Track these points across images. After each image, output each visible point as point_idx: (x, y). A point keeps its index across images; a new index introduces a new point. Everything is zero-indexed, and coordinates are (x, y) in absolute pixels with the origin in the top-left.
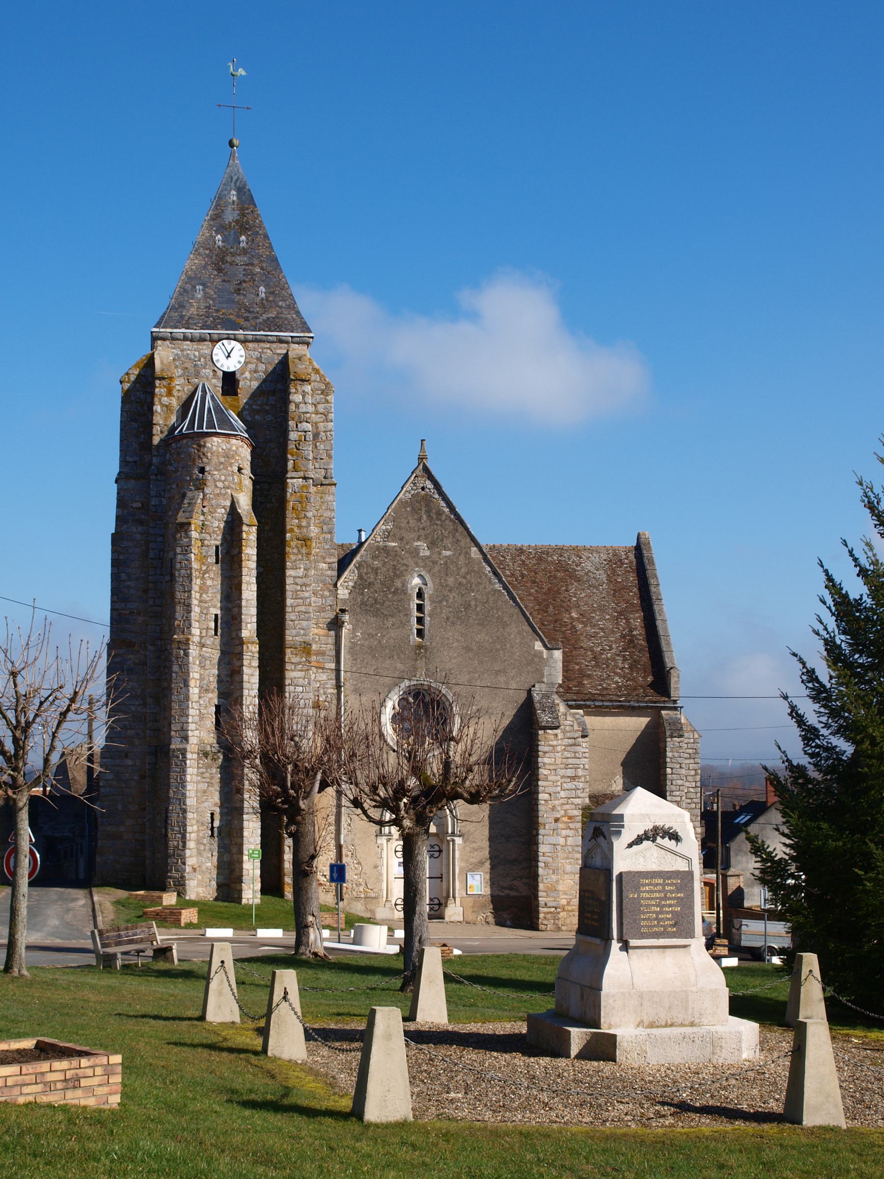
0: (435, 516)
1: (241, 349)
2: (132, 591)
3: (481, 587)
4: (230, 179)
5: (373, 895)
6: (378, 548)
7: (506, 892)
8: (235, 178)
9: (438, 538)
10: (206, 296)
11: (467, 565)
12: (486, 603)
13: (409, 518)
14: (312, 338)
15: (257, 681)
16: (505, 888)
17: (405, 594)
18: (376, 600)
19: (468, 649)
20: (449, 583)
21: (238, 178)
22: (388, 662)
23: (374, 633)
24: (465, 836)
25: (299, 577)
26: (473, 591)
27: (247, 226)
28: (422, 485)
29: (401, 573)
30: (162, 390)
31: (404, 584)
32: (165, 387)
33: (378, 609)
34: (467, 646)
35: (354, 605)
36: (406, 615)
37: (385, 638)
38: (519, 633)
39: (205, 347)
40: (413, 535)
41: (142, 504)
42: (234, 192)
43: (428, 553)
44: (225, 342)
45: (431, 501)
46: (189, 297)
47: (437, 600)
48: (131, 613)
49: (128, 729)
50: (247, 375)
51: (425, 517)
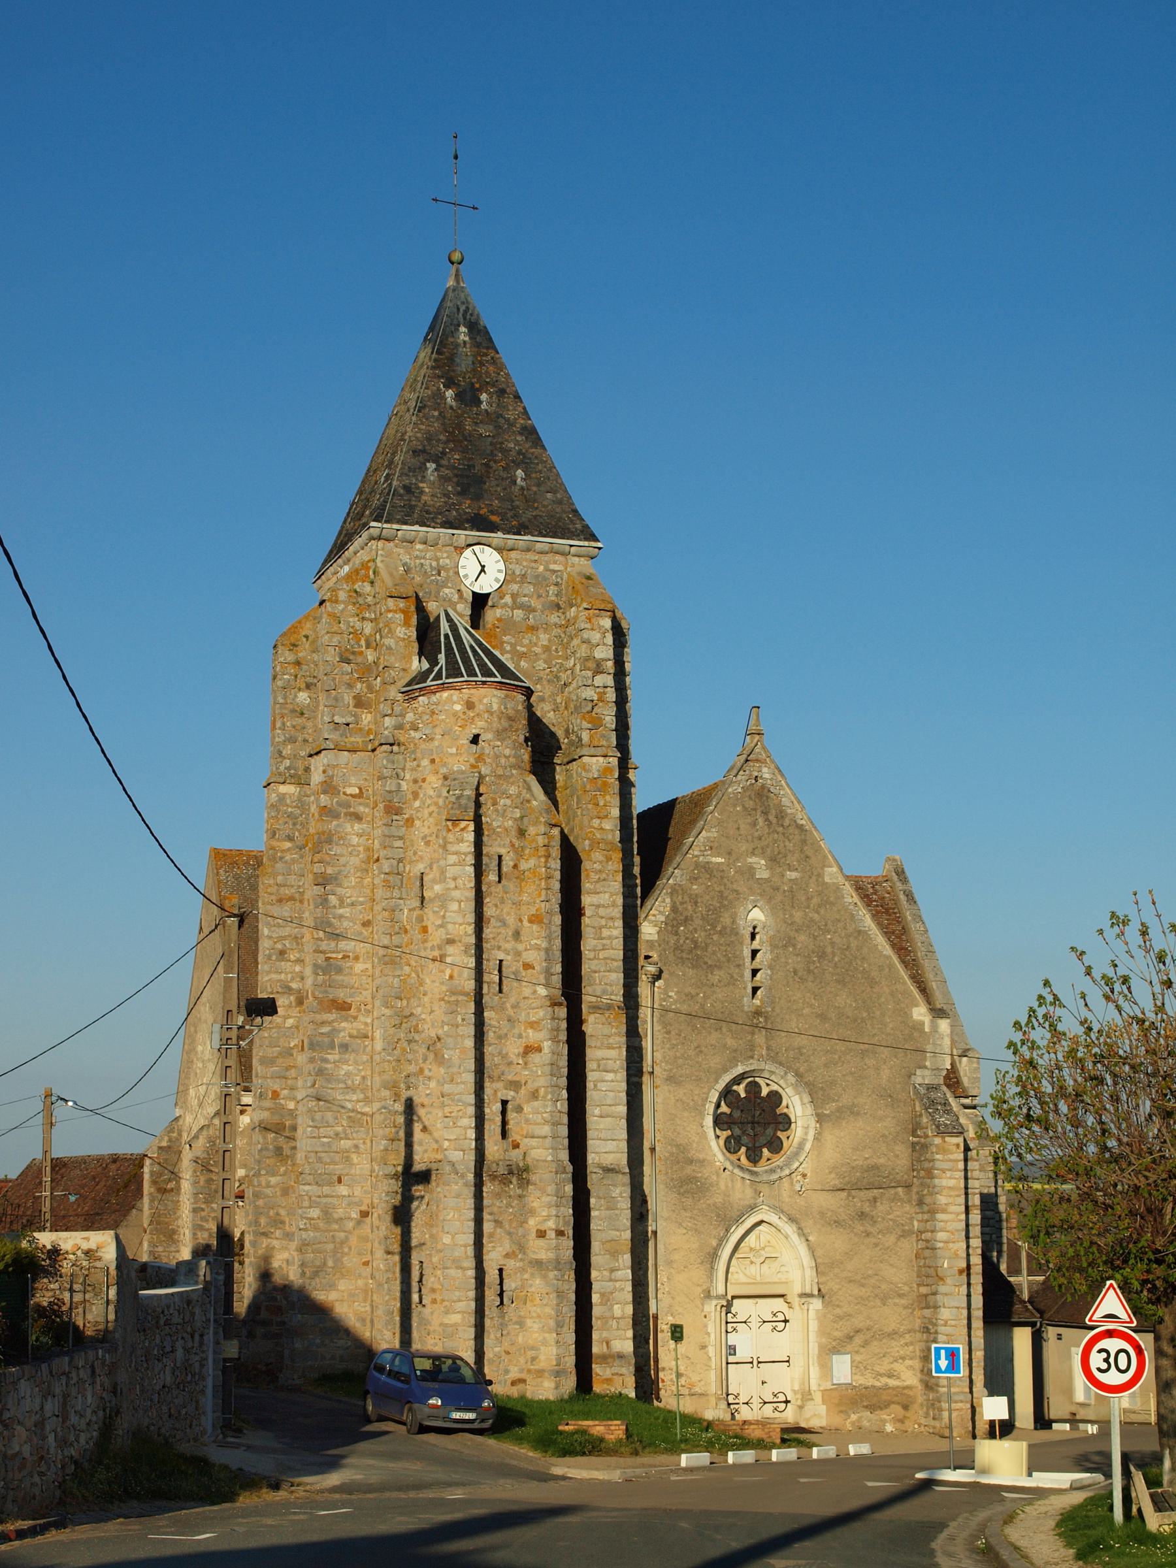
0: (774, 821)
1: (499, 561)
2: (346, 924)
3: (840, 925)
4: (455, 310)
5: (697, 1390)
6: (697, 865)
7: (885, 1380)
8: (462, 308)
9: (779, 853)
10: (444, 479)
11: (820, 893)
12: (846, 949)
13: (740, 822)
14: (600, 548)
15: (566, 1064)
16: (881, 1375)
17: (737, 934)
18: (695, 942)
19: (823, 1017)
20: (797, 920)
21: (467, 308)
22: (715, 1035)
23: (693, 992)
24: (826, 1297)
25: (604, 906)
26: (829, 932)
27: (488, 380)
28: (756, 774)
29: (731, 902)
30: (397, 616)
31: (734, 922)
32: (402, 611)
33: (699, 957)
34: (823, 1014)
35: (665, 950)
36: (739, 966)
37: (709, 1001)
38: (892, 994)
39: (445, 555)
40: (744, 847)
41: (360, 789)
42: (463, 329)
44: (476, 548)
45: (768, 797)
46: (417, 479)
47: (781, 944)
48: (345, 957)
49: (341, 1139)
50: (508, 599)
51: (761, 821)
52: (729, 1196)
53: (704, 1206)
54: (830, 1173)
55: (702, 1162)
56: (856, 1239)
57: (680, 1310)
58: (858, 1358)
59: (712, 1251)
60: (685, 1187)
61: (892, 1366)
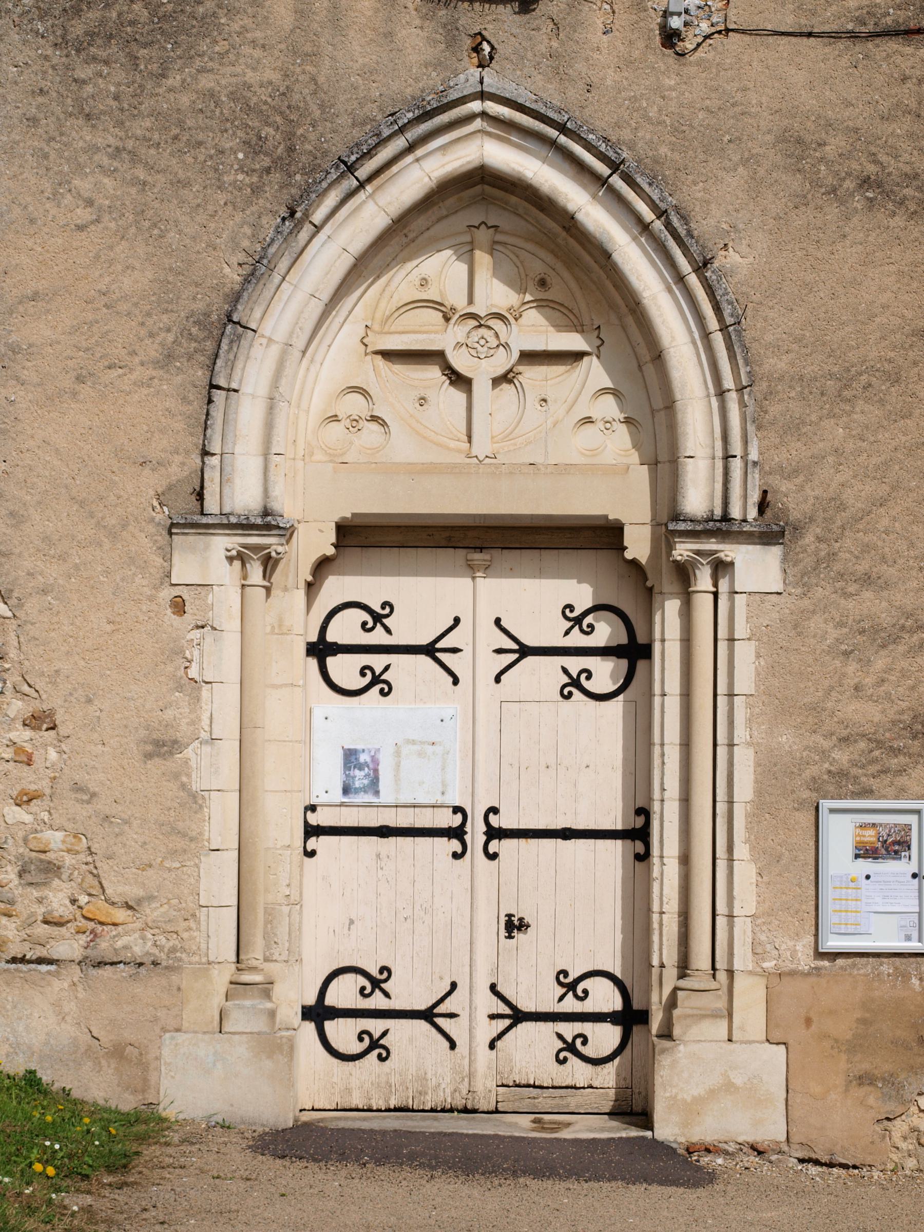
52: (313, 56)
53: (185, 100)
57: (53, 572)
59: (219, 307)
60: (93, 15)
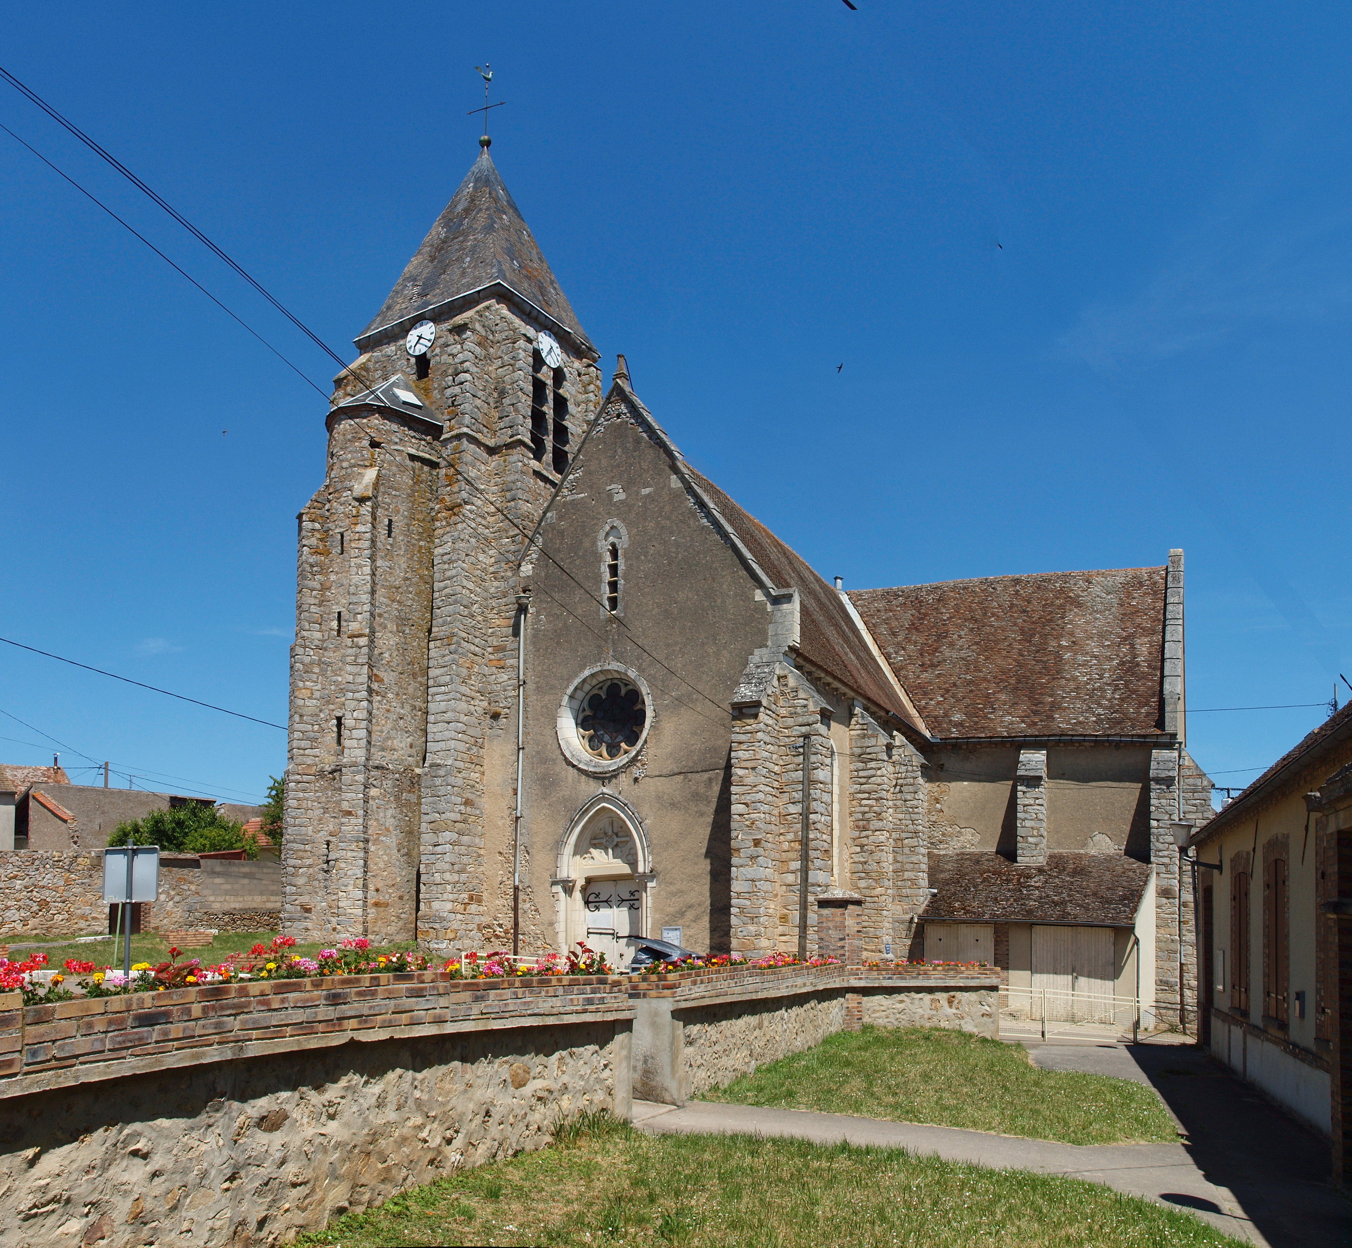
43: (622, 496)
54: (667, 759)
55: (554, 761)
56: (690, 819)
58: (689, 932)
61: (722, 939)
